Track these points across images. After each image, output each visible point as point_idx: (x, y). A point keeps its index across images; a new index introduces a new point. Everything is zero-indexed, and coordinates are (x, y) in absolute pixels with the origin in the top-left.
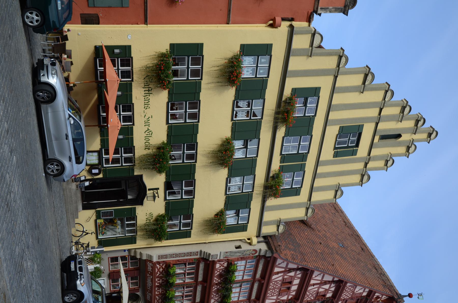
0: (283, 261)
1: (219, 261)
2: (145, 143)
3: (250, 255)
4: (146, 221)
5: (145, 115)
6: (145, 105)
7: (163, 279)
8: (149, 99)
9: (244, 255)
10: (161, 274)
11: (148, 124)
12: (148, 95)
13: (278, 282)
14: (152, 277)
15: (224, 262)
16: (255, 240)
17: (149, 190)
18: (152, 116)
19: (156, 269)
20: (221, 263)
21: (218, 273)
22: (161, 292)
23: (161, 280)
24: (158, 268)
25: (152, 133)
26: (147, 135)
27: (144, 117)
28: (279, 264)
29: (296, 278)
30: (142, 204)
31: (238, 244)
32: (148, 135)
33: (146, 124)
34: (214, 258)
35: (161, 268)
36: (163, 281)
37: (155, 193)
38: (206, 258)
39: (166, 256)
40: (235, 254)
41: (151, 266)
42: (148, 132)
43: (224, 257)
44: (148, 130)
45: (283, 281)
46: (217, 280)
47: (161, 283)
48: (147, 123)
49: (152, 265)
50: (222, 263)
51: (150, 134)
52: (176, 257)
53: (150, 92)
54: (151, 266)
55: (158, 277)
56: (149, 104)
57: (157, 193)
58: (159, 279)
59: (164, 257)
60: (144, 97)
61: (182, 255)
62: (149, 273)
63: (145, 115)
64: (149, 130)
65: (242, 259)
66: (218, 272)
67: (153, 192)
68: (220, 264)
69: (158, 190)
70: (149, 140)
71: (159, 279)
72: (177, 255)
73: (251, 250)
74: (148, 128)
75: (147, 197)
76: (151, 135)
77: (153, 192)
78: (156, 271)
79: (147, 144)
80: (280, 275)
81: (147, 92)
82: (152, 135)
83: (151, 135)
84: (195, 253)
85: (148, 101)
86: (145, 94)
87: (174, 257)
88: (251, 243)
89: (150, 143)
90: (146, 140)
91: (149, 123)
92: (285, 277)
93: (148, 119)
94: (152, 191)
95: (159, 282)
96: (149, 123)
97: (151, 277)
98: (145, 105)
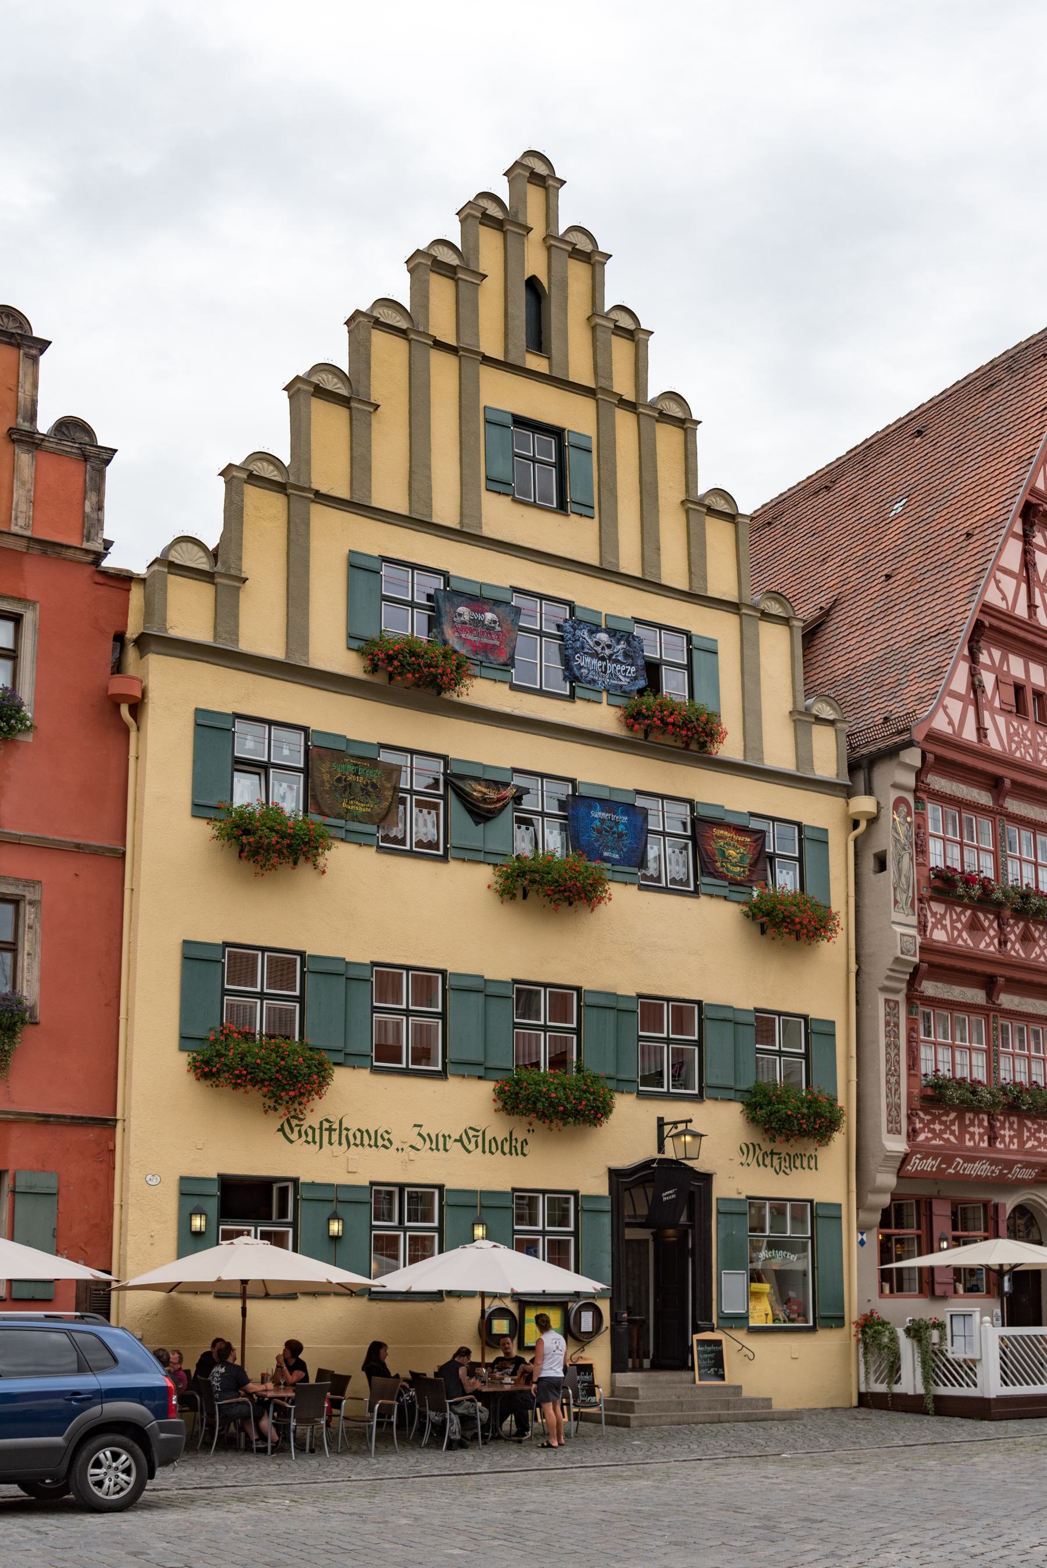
0: (941, 710)
1: (922, 927)
2: (504, 1153)
3: (910, 824)
4: (766, 1166)
5: (412, 1147)
6: (376, 1146)
7: (967, 1122)
8: (359, 1130)
9: (911, 845)
10: (953, 1128)
11: (441, 1139)
12: (344, 1133)
13: (1012, 730)
14: (958, 1159)
15: (929, 915)
16: (864, 804)
17: (661, 1148)
18: (415, 1126)
19: (933, 1142)
20: (930, 925)
21: (965, 935)
22: (1014, 1130)
23: (971, 1129)
24: (930, 1135)
25: (471, 1128)
26: (477, 1146)
27: (418, 1150)
28: (951, 723)
29: (1005, 668)
30: (707, 1178)
31: (869, 863)
32: (476, 1142)
33: (441, 1146)
34: (912, 947)
35: (932, 1126)
36: (976, 1122)
37: (674, 1131)
38: (911, 974)
39: (893, 1108)
40: (904, 872)
41: (921, 1159)
42: (470, 1142)
43: (910, 911)
44: (460, 1140)
45: (1010, 712)
46: (988, 941)
47: (982, 1130)
48: (438, 1143)
49: (919, 1156)
50: (931, 920)
51: (474, 1136)
52: (899, 1076)
53: (336, 1126)
54: (921, 1159)
55: (961, 1138)
56: (376, 1132)
57: (675, 1124)
58: (967, 1137)
59: (894, 1113)
60: (352, 1147)
61: (893, 1054)
62: (944, 1166)
63: (412, 1147)
64: (461, 1136)
65: (921, 849)
66: (960, 936)
67: (671, 1137)
68: (934, 926)
69: (665, 1121)
70: (494, 1138)
71: (967, 1137)
72: (890, 1070)
73: (895, 817)
74: (456, 1141)
75: (686, 1158)
76: (480, 1133)
77: (671, 1137)
78: (941, 1142)
79: (506, 1149)
80: (988, 723)
81: (335, 1136)
82: (477, 1128)
83: (478, 1131)
84: (888, 1010)
85: (365, 1134)
86: (340, 1144)
87: (898, 1083)
88: (870, 817)
89: (506, 1139)
90: (494, 1149)
91: (437, 1136)
92: (997, 704)
93: (425, 1140)
94: (668, 1142)
95: (977, 1137)
96: (437, 1136)
97: (959, 1163)
98: (376, 1146)
